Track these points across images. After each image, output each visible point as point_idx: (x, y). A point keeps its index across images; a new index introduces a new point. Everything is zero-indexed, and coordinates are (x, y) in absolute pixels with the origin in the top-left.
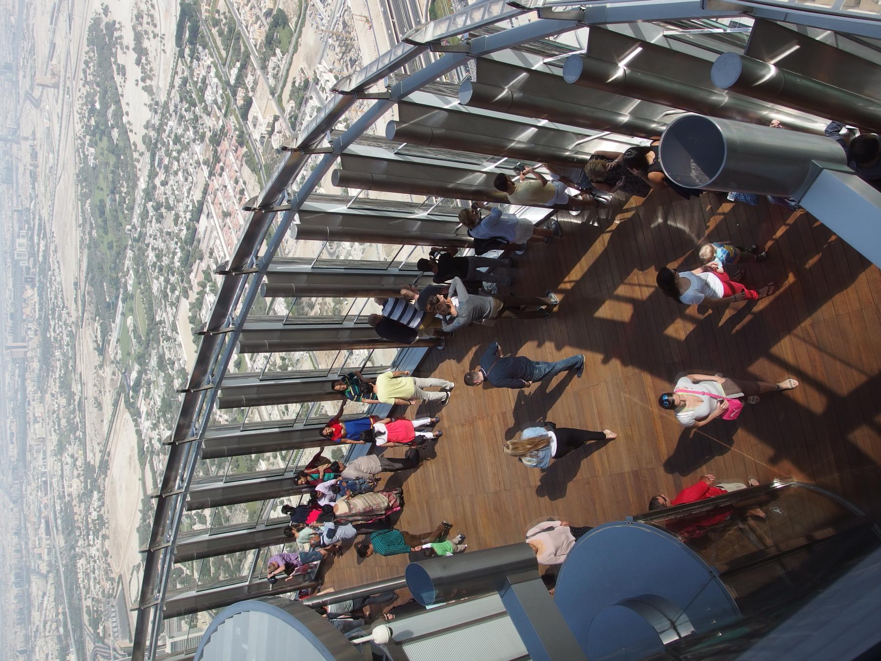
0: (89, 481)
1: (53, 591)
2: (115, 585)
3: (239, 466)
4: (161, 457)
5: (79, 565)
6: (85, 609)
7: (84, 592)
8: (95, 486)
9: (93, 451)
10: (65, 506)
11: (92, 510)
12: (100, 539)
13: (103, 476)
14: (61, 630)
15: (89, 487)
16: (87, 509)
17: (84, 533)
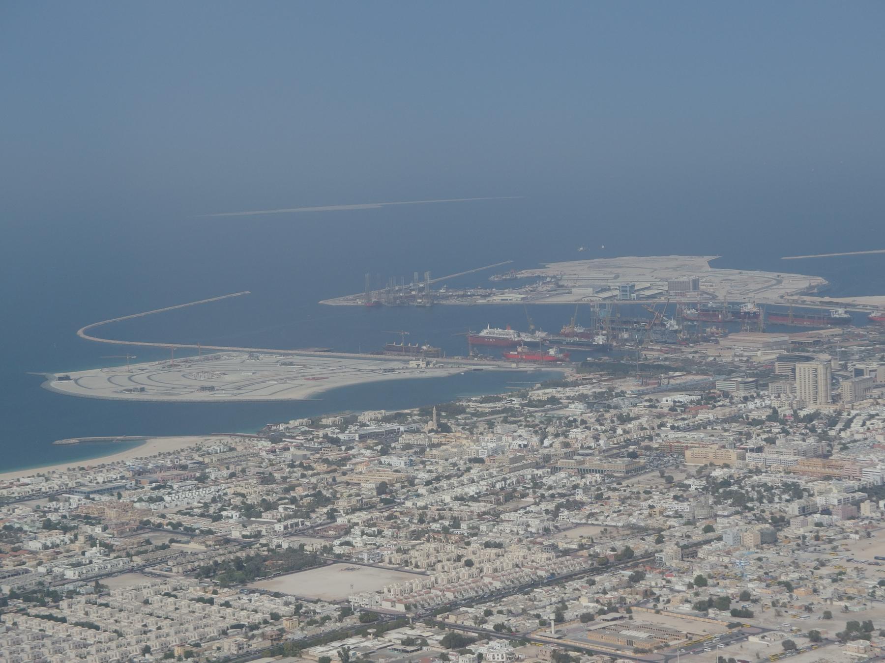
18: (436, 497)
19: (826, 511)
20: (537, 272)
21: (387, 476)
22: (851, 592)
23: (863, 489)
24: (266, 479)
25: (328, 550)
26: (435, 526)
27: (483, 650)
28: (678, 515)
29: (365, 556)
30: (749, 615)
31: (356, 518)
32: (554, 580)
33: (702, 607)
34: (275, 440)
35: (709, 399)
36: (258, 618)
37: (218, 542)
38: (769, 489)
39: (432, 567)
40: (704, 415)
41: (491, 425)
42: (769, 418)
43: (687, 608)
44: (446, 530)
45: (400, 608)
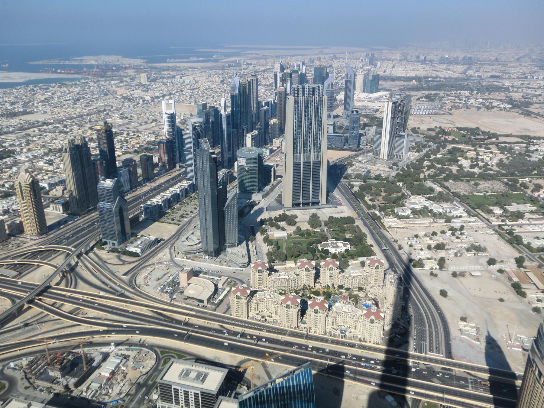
0: (520, 104)
1: (455, 77)
2: (448, 111)
3: (503, 196)
4: (524, 149)
5: (465, 92)
6: (438, 92)
7: (449, 93)
8: (514, 106)
9: (540, 108)
10: (506, 88)
11: (499, 102)
12: (479, 106)
13: (520, 112)
14: (430, 79)
15: (515, 103)
16: (501, 100)
17: (486, 97)
18: (59, 100)
19: (148, 101)
20: (82, 58)
21: (47, 96)
22: (153, 115)
23: (155, 97)
24: (16, 97)
25: (33, 111)
26: (59, 106)
27: (72, 127)
28: (115, 102)
29: (42, 112)
30: (132, 120)
31: (39, 104)
32: (88, 115)
33: (121, 119)
34: (17, 90)
35: (122, 82)
36: (16, 124)
37: (4, 110)
38: (135, 97)
39: (59, 113)
40: (121, 85)
41: (72, 87)
42: (136, 85)
43: (118, 119)
44: (62, 107)
45: (52, 121)
